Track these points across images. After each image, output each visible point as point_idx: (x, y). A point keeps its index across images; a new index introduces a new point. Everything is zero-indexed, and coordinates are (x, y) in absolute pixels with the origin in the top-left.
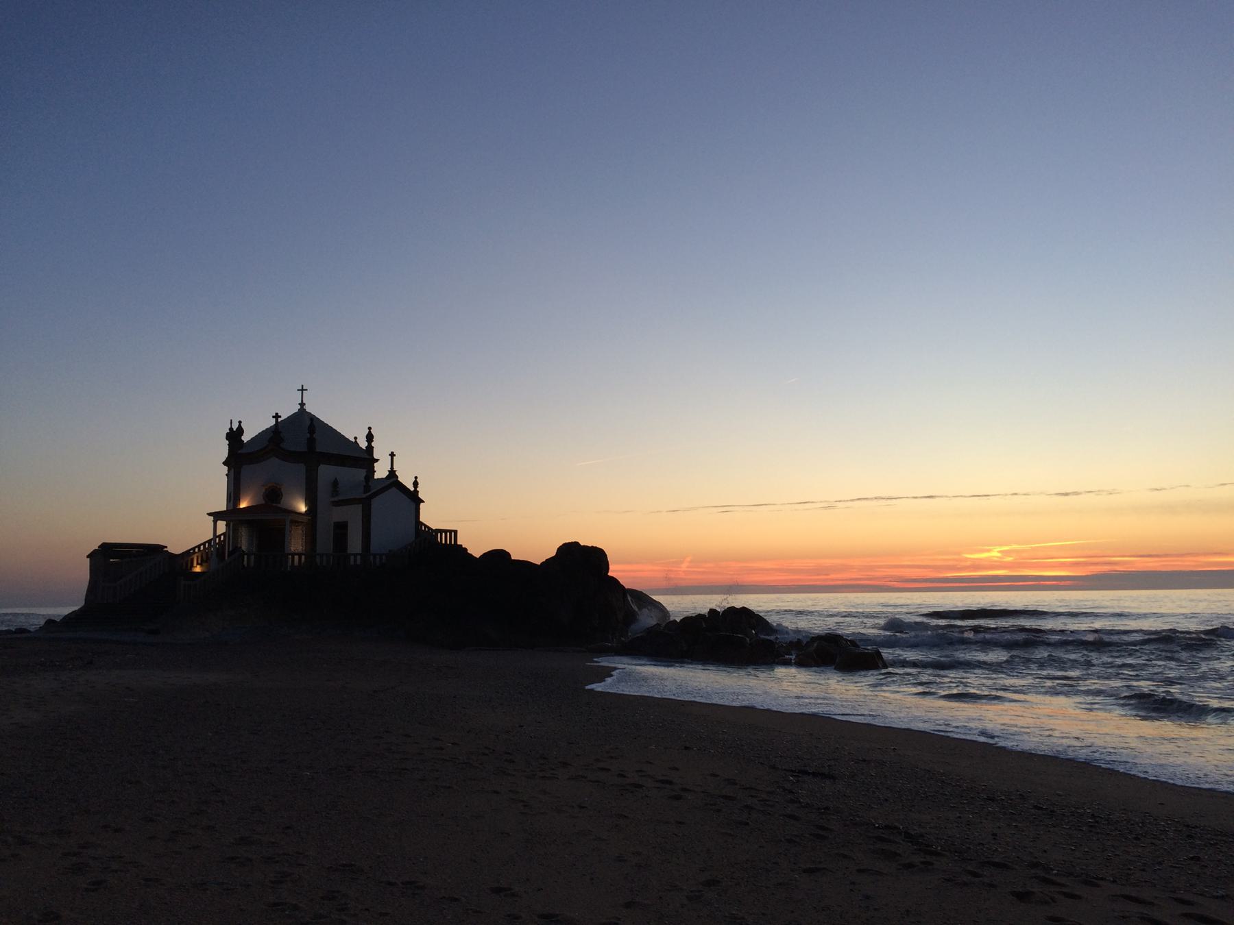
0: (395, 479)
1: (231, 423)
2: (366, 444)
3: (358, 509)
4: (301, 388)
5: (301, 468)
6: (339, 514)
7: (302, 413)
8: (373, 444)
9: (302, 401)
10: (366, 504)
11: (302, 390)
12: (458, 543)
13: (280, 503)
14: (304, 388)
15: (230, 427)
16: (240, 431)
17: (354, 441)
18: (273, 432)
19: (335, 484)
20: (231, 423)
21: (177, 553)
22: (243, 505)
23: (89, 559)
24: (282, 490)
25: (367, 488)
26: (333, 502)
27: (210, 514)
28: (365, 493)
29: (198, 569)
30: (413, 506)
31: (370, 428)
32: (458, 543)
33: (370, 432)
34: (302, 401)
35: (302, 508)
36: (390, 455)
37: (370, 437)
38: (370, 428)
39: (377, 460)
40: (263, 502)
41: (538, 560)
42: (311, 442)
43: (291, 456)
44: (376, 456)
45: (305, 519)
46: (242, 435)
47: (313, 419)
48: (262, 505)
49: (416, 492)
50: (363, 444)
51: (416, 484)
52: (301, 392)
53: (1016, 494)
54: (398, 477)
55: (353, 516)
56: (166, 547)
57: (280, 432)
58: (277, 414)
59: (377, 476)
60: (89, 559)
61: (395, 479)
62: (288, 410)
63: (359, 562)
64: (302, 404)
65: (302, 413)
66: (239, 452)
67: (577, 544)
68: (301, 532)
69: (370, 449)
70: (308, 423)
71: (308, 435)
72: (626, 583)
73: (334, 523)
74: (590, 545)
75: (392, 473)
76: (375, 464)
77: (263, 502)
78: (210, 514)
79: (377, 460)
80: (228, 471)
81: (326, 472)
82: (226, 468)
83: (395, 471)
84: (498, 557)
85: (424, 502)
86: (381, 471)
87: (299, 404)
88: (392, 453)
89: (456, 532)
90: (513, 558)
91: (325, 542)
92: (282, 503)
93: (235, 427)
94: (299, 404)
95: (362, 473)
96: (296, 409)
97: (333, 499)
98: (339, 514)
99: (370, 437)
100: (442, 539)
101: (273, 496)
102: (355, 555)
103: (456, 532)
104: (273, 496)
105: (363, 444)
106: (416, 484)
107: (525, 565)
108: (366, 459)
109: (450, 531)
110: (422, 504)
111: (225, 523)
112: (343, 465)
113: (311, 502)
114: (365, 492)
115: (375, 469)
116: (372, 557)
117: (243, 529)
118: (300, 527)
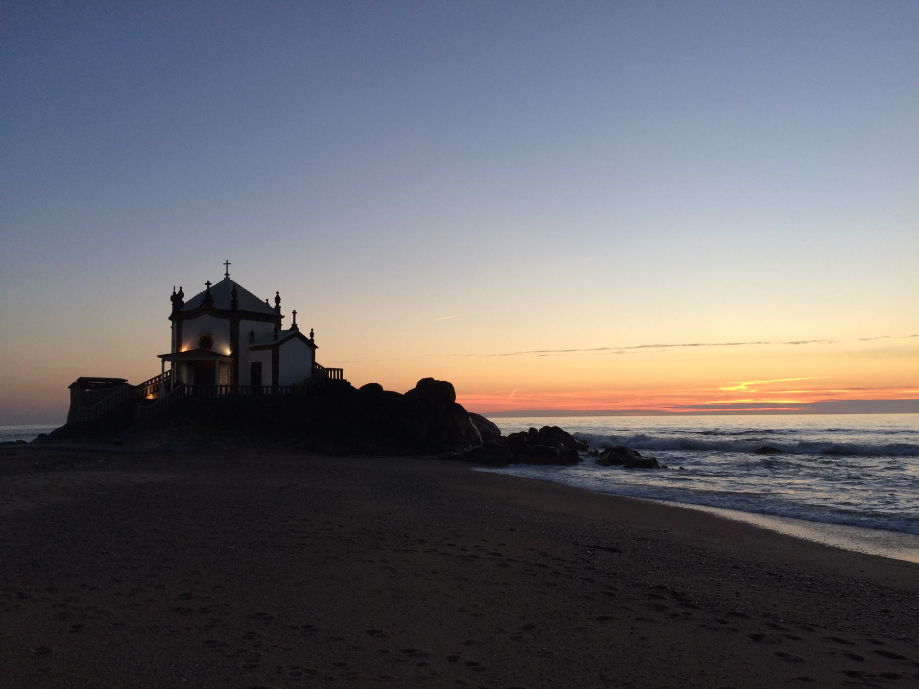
0: (297, 331)
1: (174, 288)
2: (275, 304)
4: (226, 263)
5: (227, 322)
6: (256, 356)
7: (227, 281)
8: (280, 305)
9: (227, 272)
10: (275, 349)
11: (227, 264)
12: (344, 378)
13: (211, 348)
14: (229, 263)
15: (173, 291)
16: (181, 294)
17: (266, 302)
18: (206, 295)
19: (252, 334)
20: (174, 288)
21: (135, 385)
22: (184, 350)
23: (70, 389)
24: (213, 339)
25: (276, 337)
26: (250, 348)
27: (159, 356)
28: (274, 341)
29: (151, 397)
30: (310, 351)
31: (278, 293)
32: (344, 378)
33: (278, 296)
34: (227, 272)
35: (228, 352)
36: (293, 313)
37: (278, 300)
38: (278, 293)
39: (283, 317)
40: (199, 348)
41: (403, 391)
42: (234, 303)
43: (219, 314)
44: (282, 314)
45: (230, 360)
46: (183, 297)
47: (235, 285)
48: (197, 350)
49: (312, 340)
50: (273, 304)
51: (312, 334)
52: (226, 265)
53: (759, 343)
54: (298, 329)
55: (265, 358)
56: (127, 381)
57: (211, 295)
58: (208, 282)
59: (283, 328)
60: (70, 389)
61: (297, 331)
62: (216, 279)
63: (270, 392)
64: (227, 275)
65: (227, 281)
66: (181, 310)
67: (431, 379)
68: (227, 370)
69: (278, 308)
70: (231, 288)
72: (468, 408)
73: (252, 363)
74: (442, 380)
75: (294, 326)
76: (282, 320)
77: (199, 348)
78: (159, 356)
79: (283, 317)
81: (245, 326)
83: (297, 325)
84: (373, 389)
85: (318, 348)
86: (286, 325)
87: (225, 274)
88: (294, 311)
89: (342, 370)
90: (384, 390)
91: (245, 378)
92: (212, 347)
93: (177, 291)
94: (225, 274)
95: (271, 326)
96: (223, 278)
97: (249, 346)
98: (256, 356)
99: (278, 300)
100: (332, 375)
101: (206, 343)
102: (267, 387)
103: (342, 370)
104: (206, 343)
105: (273, 304)
106: (312, 334)
108: (275, 316)
109: (338, 370)
110: (316, 349)
111: (170, 363)
112: (258, 320)
114: (275, 340)
115: (282, 323)
116: (280, 389)
117: (184, 367)
118: (227, 366)
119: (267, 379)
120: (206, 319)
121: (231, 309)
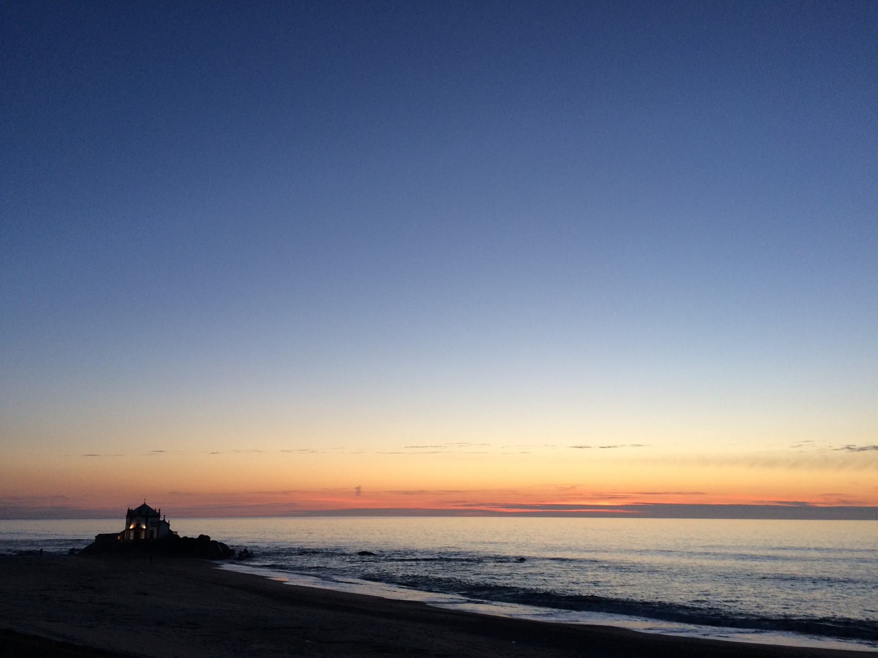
8: (161, 512)
10: (158, 527)
35: (144, 527)
37: (159, 510)
49: (169, 523)
50: (158, 511)
51: (169, 521)
55: (155, 529)
69: (159, 513)
84: (185, 538)
86: (162, 519)
96: (143, 503)
99: (159, 510)
106: (169, 521)
107: (192, 539)
108: (158, 515)
113: (146, 526)
119: (155, 536)
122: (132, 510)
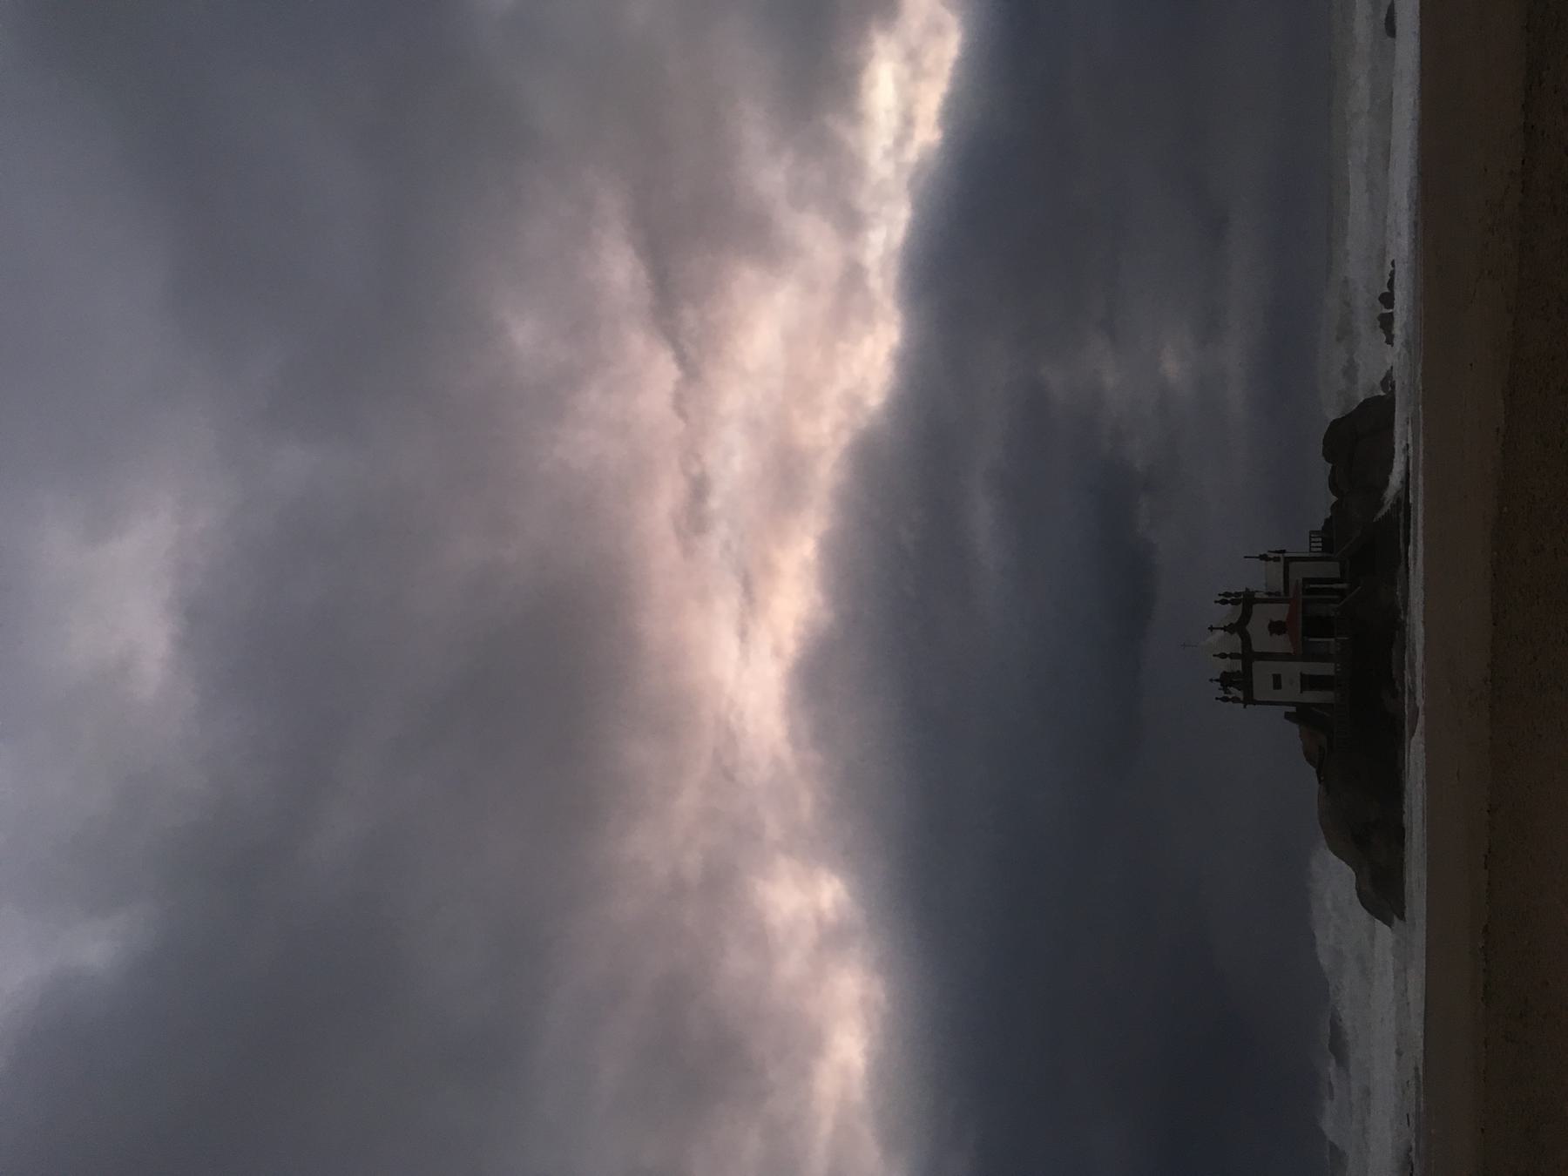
1: (1211, 680)
3: (1292, 565)
5: (1256, 607)
10: (1288, 560)
20: (1211, 680)
33: (1223, 595)
39: (1247, 589)
43: (1246, 616)
69: (1238, 594)
71: (1229, 604)
79: (1247, 589)
80: (1250, 704)
82: (1248, 706)
84: (1334, 486)
88: (1246, 557)
97: (1283, 594)
99: (1227, 594)
103: (1312, 532)
120: (1249, 628)
121: (1241, 604)
122: (1223, 656)
